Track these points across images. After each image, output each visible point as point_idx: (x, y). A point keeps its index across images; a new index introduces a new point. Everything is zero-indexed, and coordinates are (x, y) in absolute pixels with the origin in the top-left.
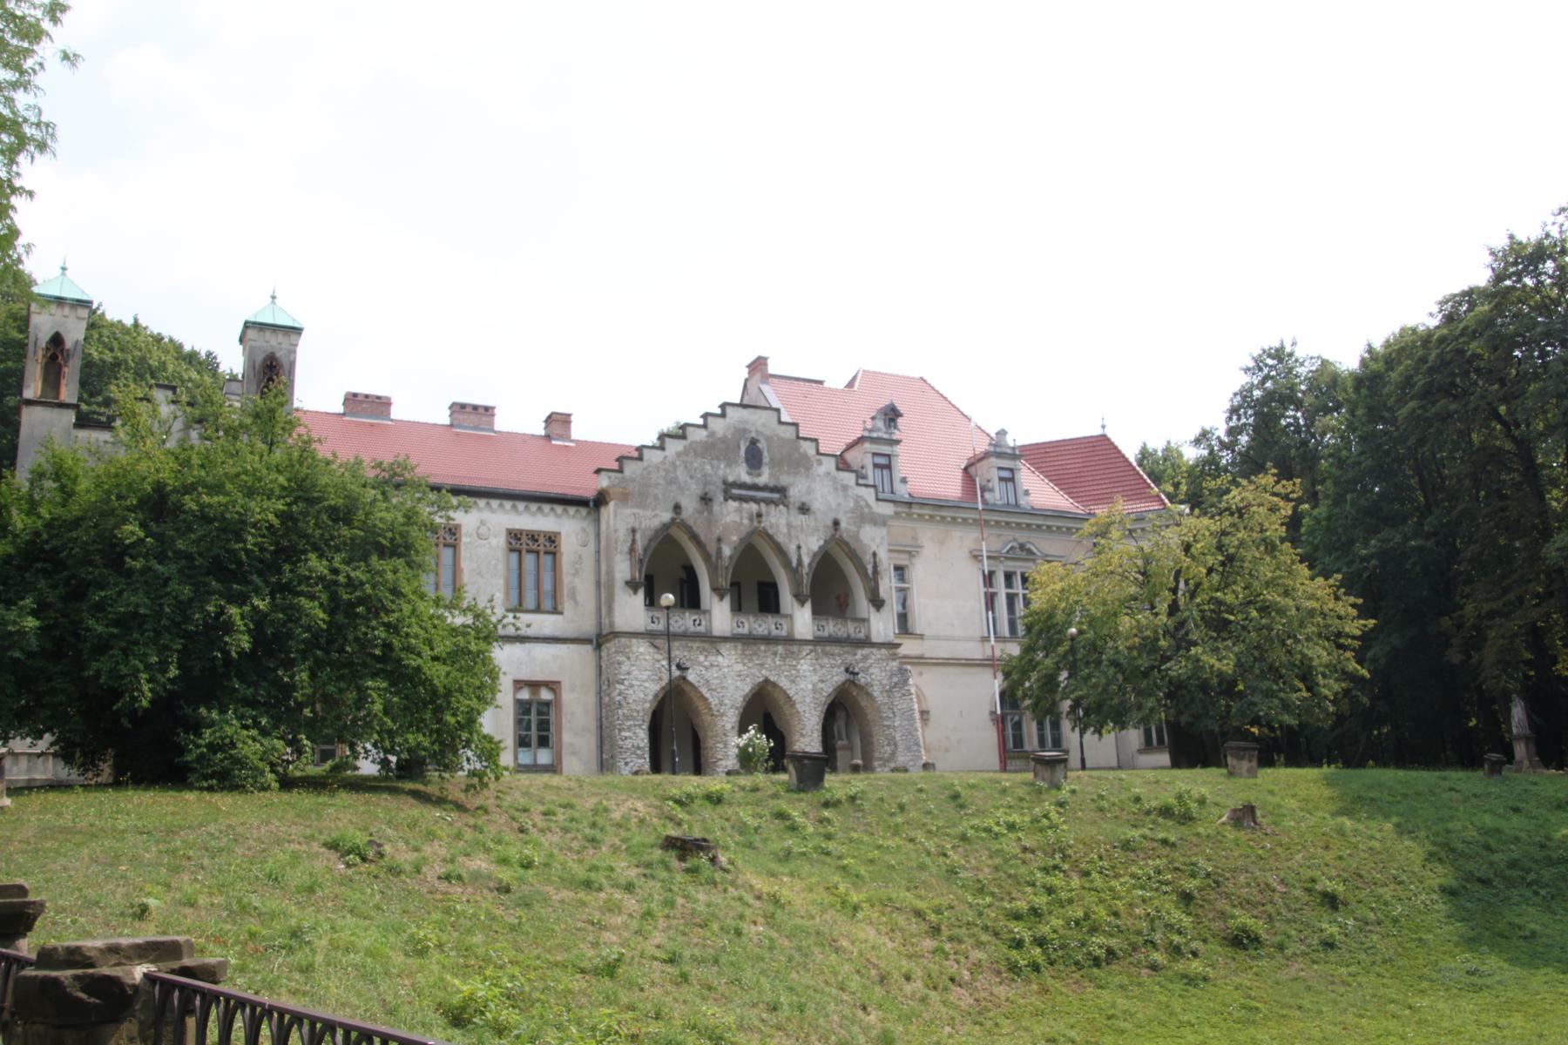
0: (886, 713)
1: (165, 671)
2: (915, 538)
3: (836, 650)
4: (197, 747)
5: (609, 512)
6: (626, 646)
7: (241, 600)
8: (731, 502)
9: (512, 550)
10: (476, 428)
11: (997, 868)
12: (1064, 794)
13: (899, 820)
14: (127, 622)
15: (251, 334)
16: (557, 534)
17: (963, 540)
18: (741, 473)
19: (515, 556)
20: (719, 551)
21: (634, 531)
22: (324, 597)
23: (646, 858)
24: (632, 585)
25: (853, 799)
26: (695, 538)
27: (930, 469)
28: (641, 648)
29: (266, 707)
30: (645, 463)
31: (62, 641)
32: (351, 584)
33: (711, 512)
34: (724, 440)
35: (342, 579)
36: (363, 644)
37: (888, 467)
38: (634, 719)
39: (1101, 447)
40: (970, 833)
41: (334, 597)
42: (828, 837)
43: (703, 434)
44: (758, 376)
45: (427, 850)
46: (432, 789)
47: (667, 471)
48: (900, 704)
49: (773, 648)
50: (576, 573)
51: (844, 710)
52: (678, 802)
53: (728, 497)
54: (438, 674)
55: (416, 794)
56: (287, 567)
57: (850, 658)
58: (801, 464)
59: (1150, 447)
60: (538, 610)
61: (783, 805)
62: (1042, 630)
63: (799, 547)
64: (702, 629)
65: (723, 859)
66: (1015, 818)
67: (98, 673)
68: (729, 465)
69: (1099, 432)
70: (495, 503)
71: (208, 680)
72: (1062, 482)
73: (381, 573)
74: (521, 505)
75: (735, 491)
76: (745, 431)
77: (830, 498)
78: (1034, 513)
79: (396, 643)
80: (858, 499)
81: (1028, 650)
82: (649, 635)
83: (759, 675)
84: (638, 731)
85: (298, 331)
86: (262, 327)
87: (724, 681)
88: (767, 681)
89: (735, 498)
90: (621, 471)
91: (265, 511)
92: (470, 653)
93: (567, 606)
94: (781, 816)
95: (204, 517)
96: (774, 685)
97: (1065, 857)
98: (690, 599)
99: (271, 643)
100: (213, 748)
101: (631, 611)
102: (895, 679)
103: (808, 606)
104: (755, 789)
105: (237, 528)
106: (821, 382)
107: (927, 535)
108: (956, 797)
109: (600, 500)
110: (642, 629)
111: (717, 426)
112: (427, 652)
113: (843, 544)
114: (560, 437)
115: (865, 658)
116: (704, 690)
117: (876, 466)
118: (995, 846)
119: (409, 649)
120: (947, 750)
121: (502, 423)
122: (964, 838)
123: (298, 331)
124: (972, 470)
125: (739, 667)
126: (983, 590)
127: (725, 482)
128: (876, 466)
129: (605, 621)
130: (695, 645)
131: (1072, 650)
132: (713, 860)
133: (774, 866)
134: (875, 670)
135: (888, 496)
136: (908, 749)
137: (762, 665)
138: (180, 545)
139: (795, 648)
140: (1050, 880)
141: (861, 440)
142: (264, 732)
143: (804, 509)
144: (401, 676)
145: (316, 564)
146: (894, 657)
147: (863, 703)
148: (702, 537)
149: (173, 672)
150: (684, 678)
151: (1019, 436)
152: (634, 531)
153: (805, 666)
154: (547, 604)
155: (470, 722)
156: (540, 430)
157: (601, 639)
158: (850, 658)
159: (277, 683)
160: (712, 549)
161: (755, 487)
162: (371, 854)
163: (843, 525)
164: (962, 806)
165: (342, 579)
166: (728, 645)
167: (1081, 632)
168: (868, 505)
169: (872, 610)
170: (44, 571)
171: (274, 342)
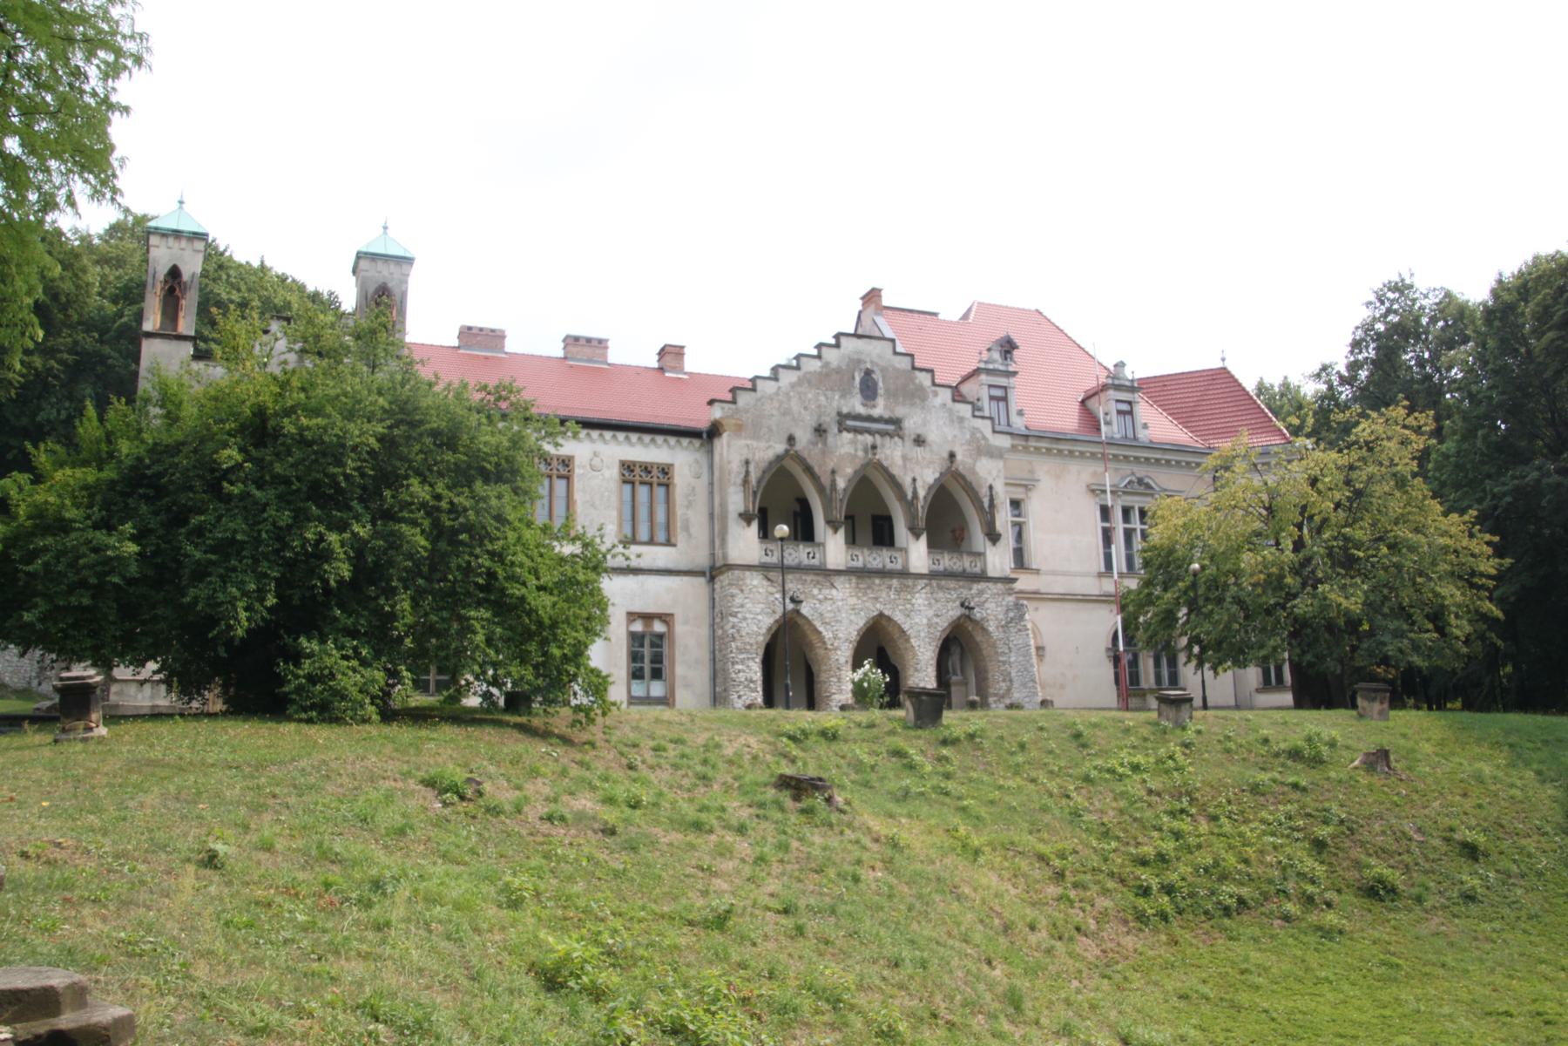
0: (1002, 648)
1: (262, 600)
2: (1032, 472)
3: (952, 584)
4: (295, 677)
5: (722, 444)
6: (739, 579)
7: (342, 527)
8: (847, 436)
9: (625, 482)
10: (589, 360)
11: (1121, 812)
12: (1190, 735)
13: (1020, 759)
14: (227, 548)
15: (363, 264)
16: (671, 466)
17: (1080, 474)
18: (856, 405)
19: (628, 488)
20: (833, 483)
21: (747, 462)
22: (426, 523)
23: (759, 798)
24: (746, 518)
25: (971, 736)
26: (809, 470)
27: (1047, 402)
28: (755, 580)
29: (368, 637)
30: (759, 394)
31: (163, 570)
32: (454, 509)
33: (825, 443)
34: (838, 371)
35: (444, 505)
36: (467, 570)
37: (1005, 399)
38: (747, 652)
39: (1222, 377)
40: (1094, 774)
41: (436, 524)
42: (948, 776)
43: (815, 365)
44: (871, 309)
45: (530, 788)
46: (536, 722)
47: (781, 403)
48: (1016, 640)
49: (888, 581)
50: (689, 505)
51: (958, 644)
52: (792, 738)
53: (842, 428)
54: (544, 604)
55: (522, 728)
56: (387, 493)
57: (965, 593)
58: (916, 395)
59: (1267, 382)
60: (651, 542)
61: (899, 742)
62: (1162, 566)
63: (914, 480)
64: (816, 562)
65: (839, 799)
66: (1139, 758)
67: (196, 599)
68: (843, 396)
69: (1219, 365)
70: (608, 434)
71: (305, 610)
72: (1183, 416)
73: (485, 499)
74: (634, 437)
75: (850, 423)
76: (859, 361)
77: (946, 430)
78: (1151, 447)
79: (501, 573)
80: (975, 431)
81: (1148, 583)
82: (763, 568)
83: (873, 609)
84: (751, 663)
85: (409, 261)
86: (374, 257)
87: (838, 616)
88: (881, 615)
89: (849, 430)
90: (734, 402)
91: (364, 434)
92: (578, 585)
93: (680, 537)
94: (898, 753)
95: (302, 442)
96: (889, 619)
97: (1192, 801)
98: (804, 532)
99: (371, 573)
100: (312, 679)
101: (745, 544)
102: (1011, 614)
103: (924, 538)
104: (871, 726)
105: (336, 452)
106: (935, 314)
107: (1044, 469)
108: (1078, 736)
109: (714, 431)
110: (756, 562)
111: (831, 356)
112: (532, 582)
113: (958, 476)
114: (673, 369)
115: (981, 593)
116: (818, 624)
117: (992, 398)
118: (1119, 788)
119: (512, 578)
120: (1062, 687)
121: (615, 356)
122: (1087, 779)
123: (409, 261)
124: (1092, 404)
125: (853, 601)
126: (1100, 525)
127: (839, 414)
128: (992, 398)
129: (718, 552)
130: (809, 578)
131: (1194, 586)
132: (829, 800)
133: (892, 806)
134: (991, 605)
135: (1003, 428)
136: (1024, 685)
137: (876, 599)
138: (278, 468)
139: (910, 582)
140: (1176, 824)
141: (977, 372)
142: (364, 663)
143: (919, 441)
144: (506, 607)
145: (418, 490)
146: (1010, 592)
147: (979, 638)
148: (816, 469)
149: (271, 601)
150: (798, 612)
151: (1137, 370)
152: (747, 462)
153: (920, 600)
154: (661, 536)
155: (579, 652)
156: (653, 363)
157: (714, 572)
158: (965, 593)
159: (378, 612)
160: (826, 481)
161: (870, 419)
162: (469, 793)
163: (959, 457)
164: (1084, 746)
165: (444, 505)
166: (842, 578)
167: (1203, 568)
168: (984, 438)
169: (988, 544)
170: (147, 498)
171: (384, 273)
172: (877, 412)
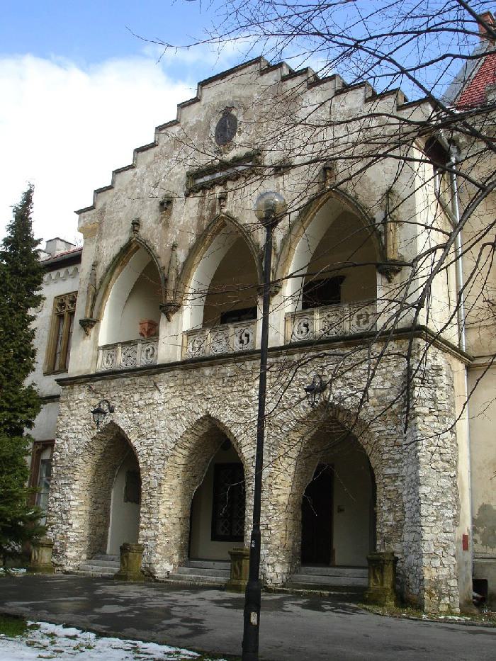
88: (209, 416)
125: (176, 402)
161: (224, 166)
172: (229, 156)
